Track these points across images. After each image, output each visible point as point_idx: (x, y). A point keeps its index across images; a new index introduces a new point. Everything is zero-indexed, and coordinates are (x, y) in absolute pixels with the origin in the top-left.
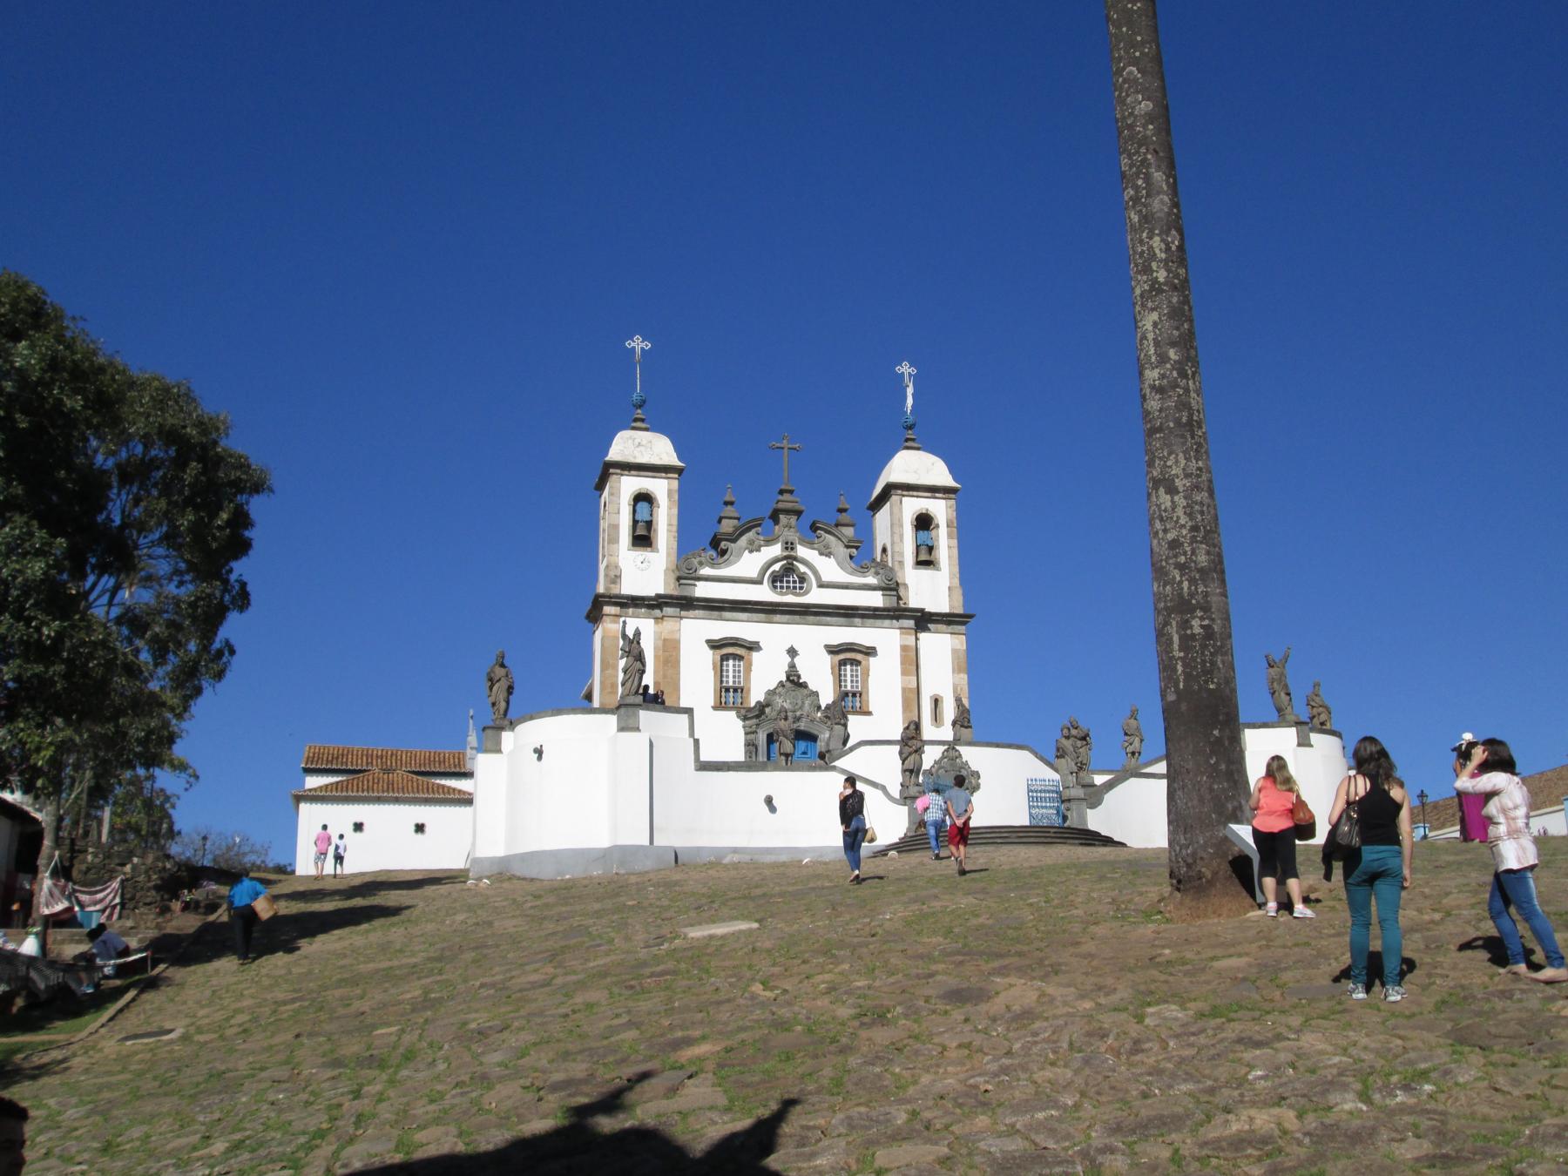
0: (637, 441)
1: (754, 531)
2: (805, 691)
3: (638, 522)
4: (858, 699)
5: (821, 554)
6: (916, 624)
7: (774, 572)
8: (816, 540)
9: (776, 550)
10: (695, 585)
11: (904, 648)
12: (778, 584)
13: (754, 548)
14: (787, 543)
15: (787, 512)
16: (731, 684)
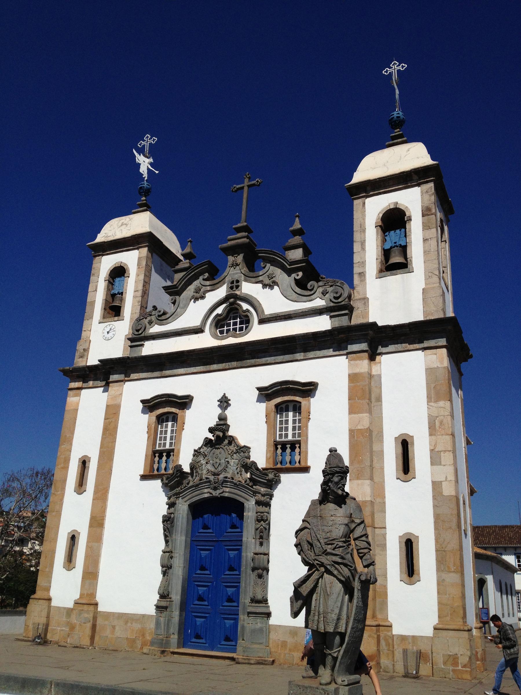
0: (120, 224)
1: (201, 278)
2: (232, 448)
3: (115, 294)
4: (297, 450)
5: (265, 286)
6: (370, 346)
7: (218, 315)
8: (261, 273)
9: (222, 292)
10: (142, 345)
11: (353, 378)
12: (225, 328)
13: (199, 296)
14: (232, 282)
15: (233, 250)
16: (167, 447)
